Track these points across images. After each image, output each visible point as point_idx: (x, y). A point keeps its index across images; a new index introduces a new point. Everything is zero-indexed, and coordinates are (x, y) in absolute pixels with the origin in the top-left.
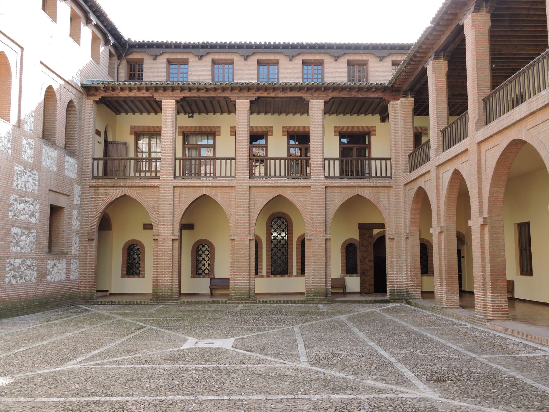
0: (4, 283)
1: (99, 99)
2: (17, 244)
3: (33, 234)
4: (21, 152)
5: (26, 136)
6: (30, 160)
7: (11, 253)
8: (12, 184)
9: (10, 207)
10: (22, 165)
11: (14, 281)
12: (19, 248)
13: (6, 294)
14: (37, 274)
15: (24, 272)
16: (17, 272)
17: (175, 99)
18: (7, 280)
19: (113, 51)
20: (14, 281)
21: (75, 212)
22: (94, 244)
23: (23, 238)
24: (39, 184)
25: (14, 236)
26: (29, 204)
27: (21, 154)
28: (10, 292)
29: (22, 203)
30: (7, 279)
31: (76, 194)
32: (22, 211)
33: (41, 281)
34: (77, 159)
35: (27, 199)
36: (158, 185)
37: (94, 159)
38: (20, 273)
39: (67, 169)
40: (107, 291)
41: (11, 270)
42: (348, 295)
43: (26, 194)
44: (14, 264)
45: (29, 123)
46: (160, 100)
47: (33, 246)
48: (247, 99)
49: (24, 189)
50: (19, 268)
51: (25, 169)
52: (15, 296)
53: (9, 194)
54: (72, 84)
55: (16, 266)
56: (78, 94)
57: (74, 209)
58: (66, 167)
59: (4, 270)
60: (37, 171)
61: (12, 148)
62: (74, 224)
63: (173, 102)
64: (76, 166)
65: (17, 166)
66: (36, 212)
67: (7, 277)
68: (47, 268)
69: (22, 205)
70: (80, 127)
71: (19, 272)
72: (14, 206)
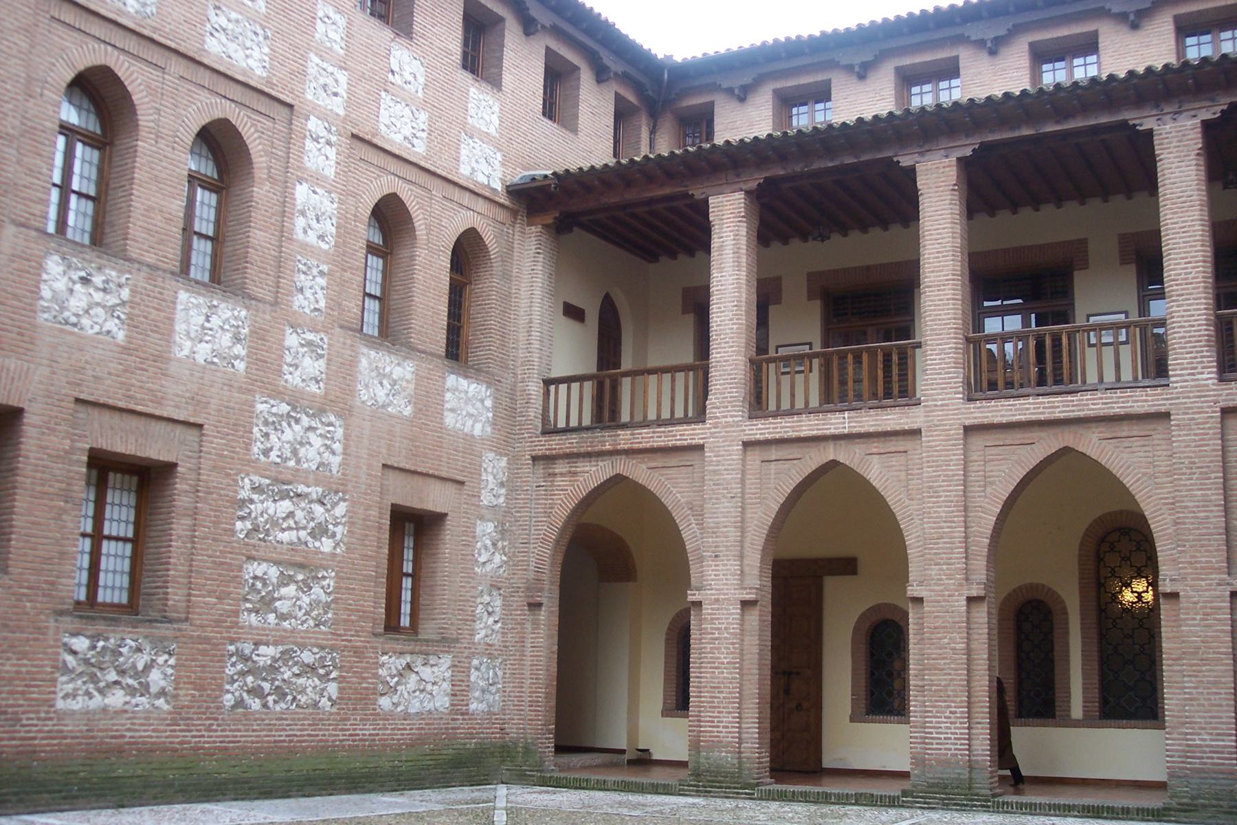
0: (218, 708)
1: (555, 218)
2: (267, 604)
3: (325, 583)
4: (280, 366)
5: (300, 326)
6: (313, 388)
7: (242, 628)
8: (248, 450)
9: (241, 508)
10: (283, 400)
11: (256, 704)
12: (271, 618)
13: (227, 736)
14: (341, 690)
15: (290, 683)
16: (264, 679)
17: (744, 187)
18: (228, 700)
19: (631, 98)
20: (256, 704)
21: (486, 529)
22: (548, 617)
23: (290, 590)
24: (345, 449)
25: (253, 585)
26: (311, 502)
27: (280, 371)
28: (239, 730)
29: (282, 499)
30: (229, 696)
31: (490, 478)
32: (284, 519)
33: (354, 709)
34: (492, 381)
35: (301, 488)
36: (701, 442)
37: (548, 382)
38: (277, 683)
39: (452, 410)
40: (623, 752)
41: (243, 674)
42: (825, 780)
43: (298, 475)
44: (255, 658)
45: (308, 293)
46: (703, 196)
47: (326, 613)
48: (947, 156)
49: (292, 463)
50: (273, 669)
51: (294, 409)
52: (257, 742)
53: (237, 474)
54: (472, 186)
55: (261, 663)
56: (501, 215)
57: (482, 518)
58: (447, 406)
59: (217, 672)
60: (338, 416)
61: (248, 357)
62: (482, 559)
63: (740, 196)
64: (489, 403)
65: (266, 402)
66: (336, 525)
67: (228, 691)
68: (376, 676)
69: (286, 506)
70: (507, 297)
71: (274, 680)
72: (252, 507)
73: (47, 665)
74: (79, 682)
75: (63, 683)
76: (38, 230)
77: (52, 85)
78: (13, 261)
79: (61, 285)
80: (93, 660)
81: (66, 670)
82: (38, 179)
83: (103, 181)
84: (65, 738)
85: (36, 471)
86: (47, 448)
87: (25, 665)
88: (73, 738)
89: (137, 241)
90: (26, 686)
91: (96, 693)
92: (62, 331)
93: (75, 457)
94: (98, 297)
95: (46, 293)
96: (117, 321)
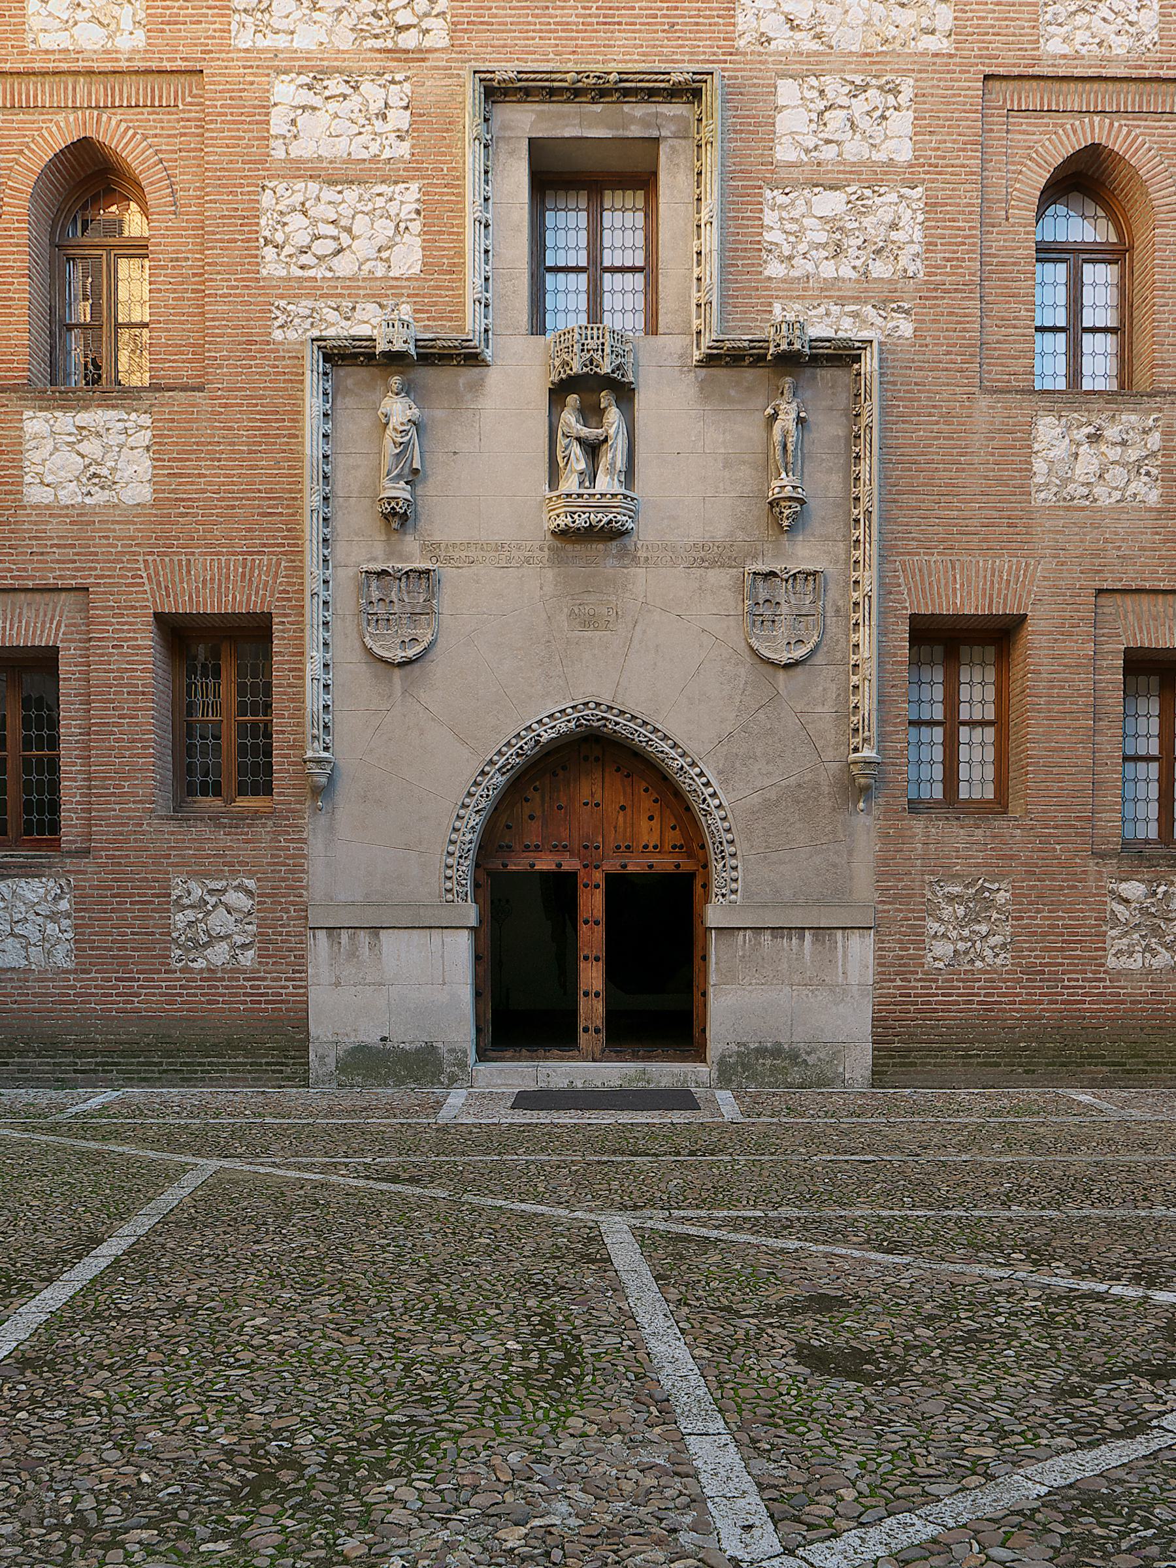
73: (1090, 917)
74: (1136, 936)
75: (1114, 939)
76: (1023, 392)
77: (1021, 200)
78: (993, 438)
79: (1061, 450)
80: (1153, 910)
81: (1115, 921)
82: (1015, 327)
83: (1126, 303)
84: (1123, 1002)
85: (1052, 687)
86: (1062, 656)
87: (1063, 918)
88: (1132, 1002)
89: (1169, 366)
90: (1064, 941)
91: (1159, 949)
92: (1068, 508)
93: (1105, 663)
94: (1114, 453)
95: (1039, 466)
96: (1146, 479)
